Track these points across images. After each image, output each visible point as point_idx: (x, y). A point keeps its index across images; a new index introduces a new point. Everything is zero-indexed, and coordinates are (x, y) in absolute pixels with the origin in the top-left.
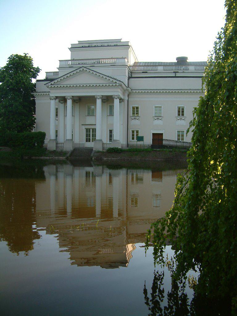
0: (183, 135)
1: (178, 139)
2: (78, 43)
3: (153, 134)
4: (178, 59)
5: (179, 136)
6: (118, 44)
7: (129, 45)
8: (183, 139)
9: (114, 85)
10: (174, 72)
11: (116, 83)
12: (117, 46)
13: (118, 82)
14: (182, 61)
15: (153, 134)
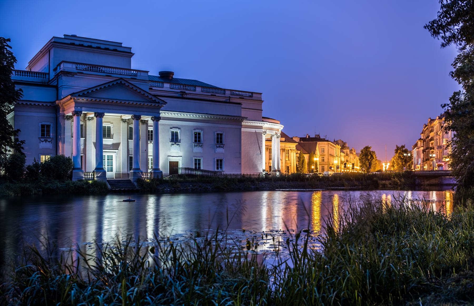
0: (199, 164)
1: (196, 167)
2: (63, 37)
3: (170, 162)
4: (161, 73)
5: (196, 164)
6: (119, 49)
7: (132, 51)
8: (199, 167)
9: (157, 105)
10: (181, 92)
11: (159, 103)
12: (115, 50)
13: (161, 102)
14: (166, 76)
15: (170, 162)
